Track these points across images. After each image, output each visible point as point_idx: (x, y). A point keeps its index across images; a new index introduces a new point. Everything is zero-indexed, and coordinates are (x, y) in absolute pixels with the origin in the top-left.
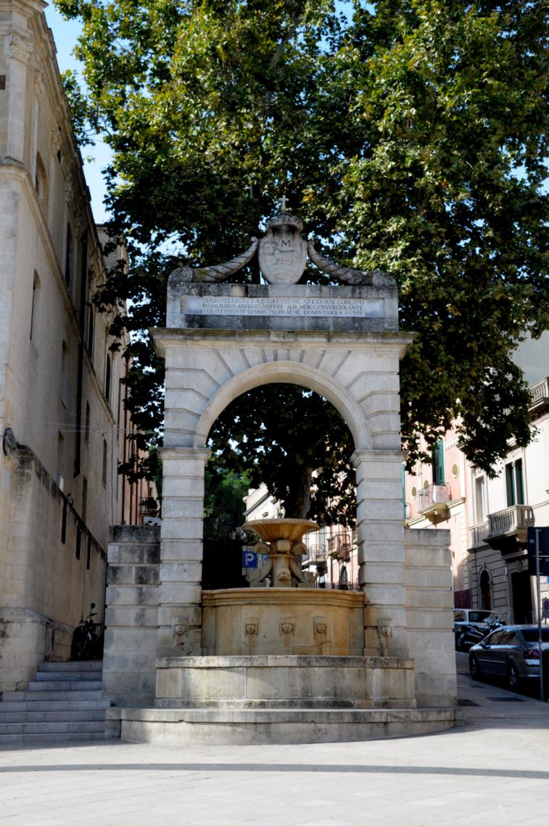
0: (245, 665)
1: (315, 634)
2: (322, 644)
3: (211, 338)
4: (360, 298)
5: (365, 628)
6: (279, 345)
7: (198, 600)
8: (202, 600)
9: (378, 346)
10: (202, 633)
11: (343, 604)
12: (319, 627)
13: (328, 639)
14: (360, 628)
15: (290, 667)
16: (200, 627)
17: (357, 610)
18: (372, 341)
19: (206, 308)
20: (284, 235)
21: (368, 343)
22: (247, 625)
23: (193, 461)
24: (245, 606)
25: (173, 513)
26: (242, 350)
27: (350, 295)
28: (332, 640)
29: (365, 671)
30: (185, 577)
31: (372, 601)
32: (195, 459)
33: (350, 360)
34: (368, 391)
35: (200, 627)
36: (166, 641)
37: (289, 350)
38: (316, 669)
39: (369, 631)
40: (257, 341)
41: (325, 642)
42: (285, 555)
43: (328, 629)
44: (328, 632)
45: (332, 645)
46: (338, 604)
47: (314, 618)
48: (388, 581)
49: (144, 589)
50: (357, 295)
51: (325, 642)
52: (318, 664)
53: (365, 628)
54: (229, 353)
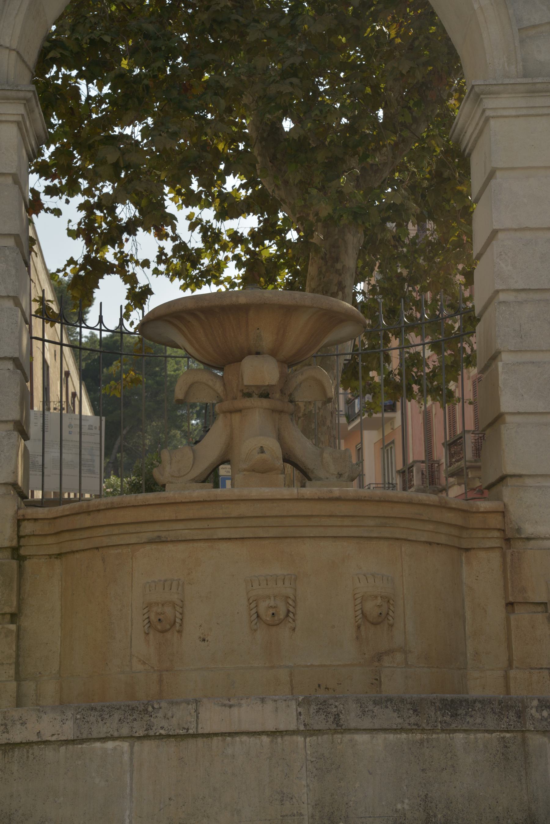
0: (125, 731)
2: (379, 657)
8: (19, 537)
11: (443, 539)
15: (274, 734)
16: (14, 617)
22: (149, 606)
24: (148, 547)
29: (524, 742)
31: (529, 529)
38: (362, 738)
41: (390, 652)
42: (265, 403)
46: (425, 537)
51: (390, 652)
52: (367, 723)
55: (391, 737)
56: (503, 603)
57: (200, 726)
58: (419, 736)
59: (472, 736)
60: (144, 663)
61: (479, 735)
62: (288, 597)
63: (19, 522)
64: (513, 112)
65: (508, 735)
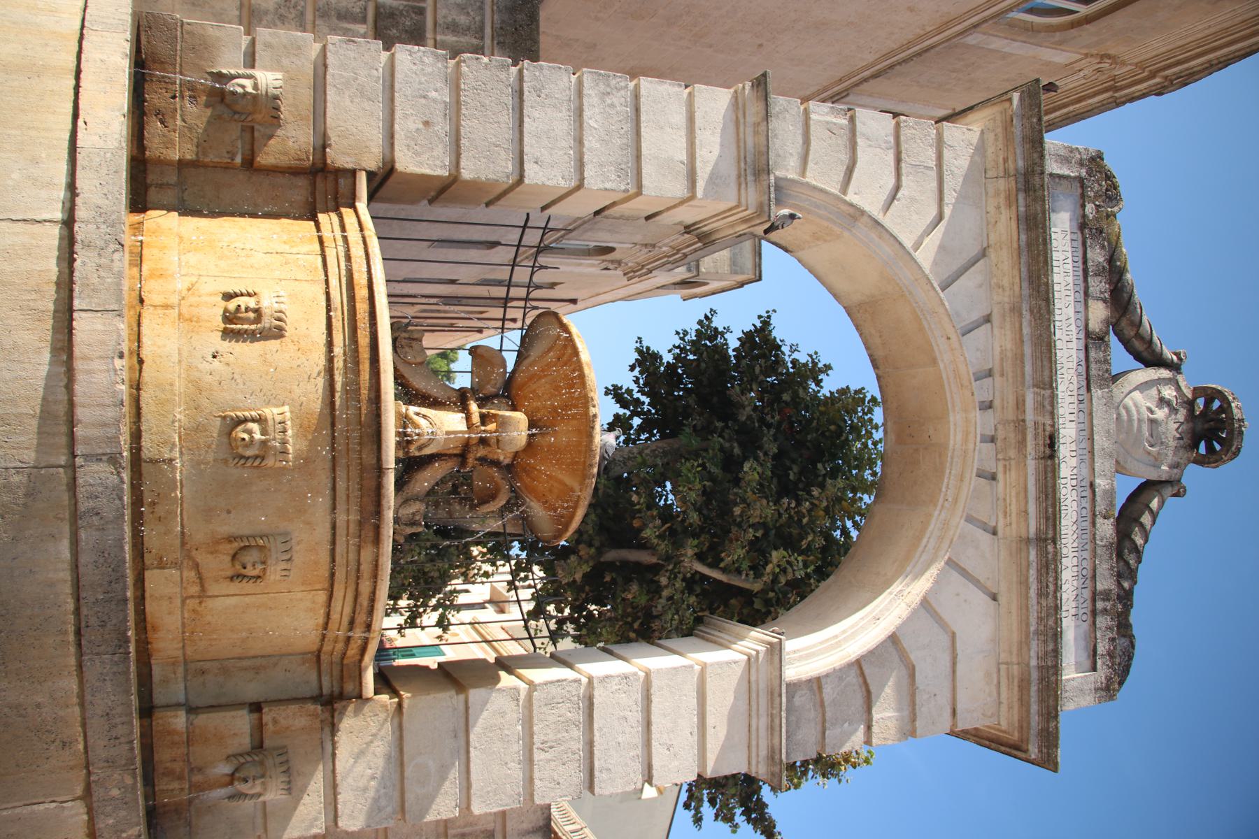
1: (231, 539)
3: (1023, 237)
4: (1094, 613)
5: (256, 707)
6: (1010, 414)
7: (339, 157)
8: (339, 172)
9: (1015, 670)
10: (227, 167)
12: (251, 557)
13: (213, 589)
14: (253, 691)
17: (313, 676)
18: (1033, 654)
19: (1060, 236)
20: (1190, 425)
21: (1024, 643)
23: (734, 174)
25: (595, 100)
26: (987, 319)
27: (1099, 587)
28: (210, 603)
30: (406, 125)
32: (741, 178)
33: (980, 599)
34: (914, 657)
35: (249, 163)
36: (202, 47)
37: (993, 440)
39: (241, 722)
40: (1019, 358)
43: (248, 586)
44: (234, 587)
45: (191, 603)
47: (286, 538)
48: (409, 771)
49: (362, 28)
50: (1100, 605)
53: (256, 707)
54: (980, 286)
55: (67, 589)
56: (261, 700)
57: (83, 314)
58: (71, 629)
59: (75, 700)
60: (189, 290)
61: (77, 710)
62: (263, 458)
63: (353, 173)
64: (753, 678)
65: (81, 747)
